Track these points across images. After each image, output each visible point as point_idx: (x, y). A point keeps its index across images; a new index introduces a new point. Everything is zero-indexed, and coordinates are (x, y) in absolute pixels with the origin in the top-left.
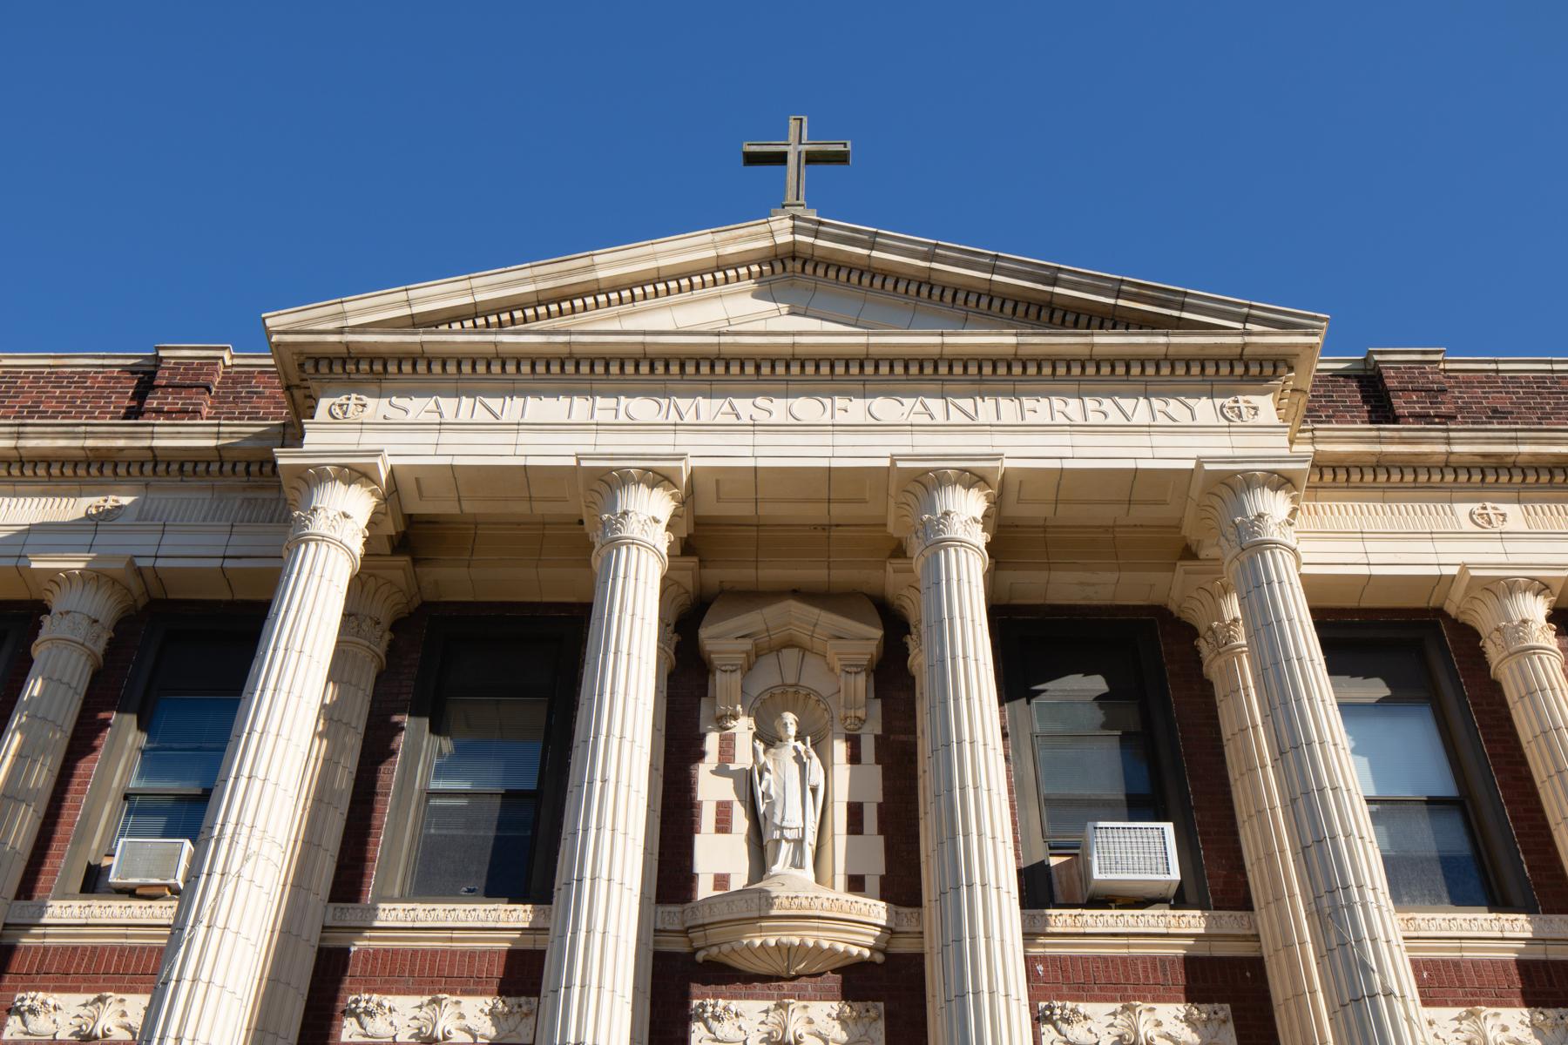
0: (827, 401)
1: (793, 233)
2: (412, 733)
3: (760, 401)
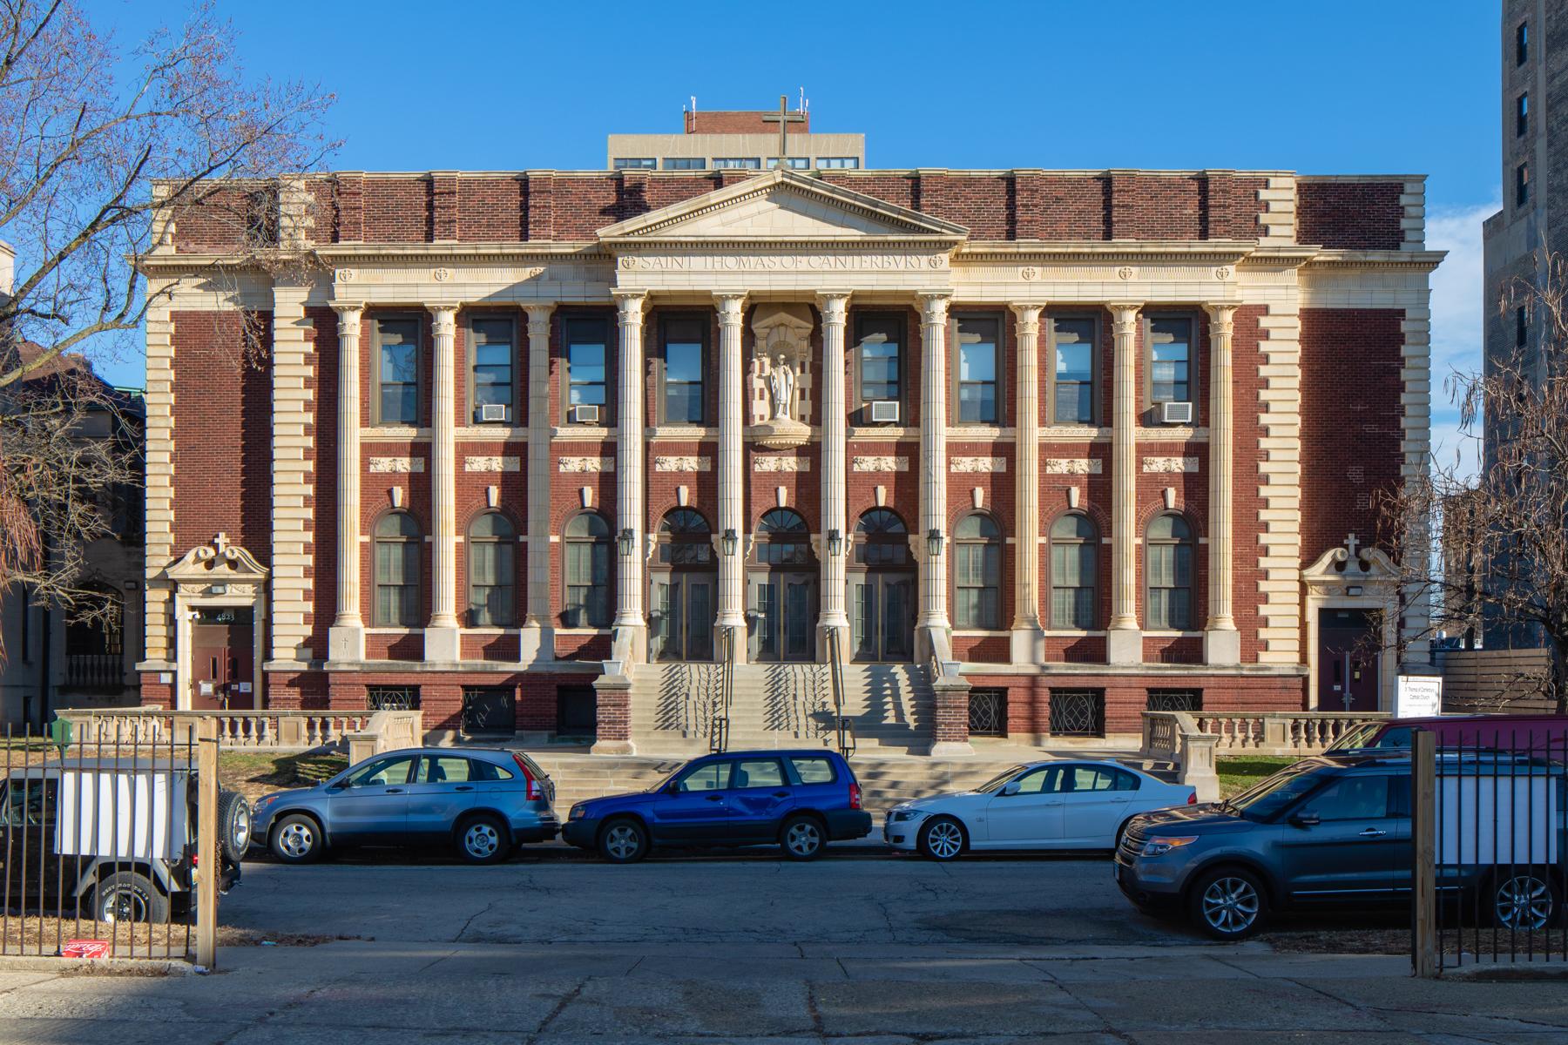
2: (656, 363)
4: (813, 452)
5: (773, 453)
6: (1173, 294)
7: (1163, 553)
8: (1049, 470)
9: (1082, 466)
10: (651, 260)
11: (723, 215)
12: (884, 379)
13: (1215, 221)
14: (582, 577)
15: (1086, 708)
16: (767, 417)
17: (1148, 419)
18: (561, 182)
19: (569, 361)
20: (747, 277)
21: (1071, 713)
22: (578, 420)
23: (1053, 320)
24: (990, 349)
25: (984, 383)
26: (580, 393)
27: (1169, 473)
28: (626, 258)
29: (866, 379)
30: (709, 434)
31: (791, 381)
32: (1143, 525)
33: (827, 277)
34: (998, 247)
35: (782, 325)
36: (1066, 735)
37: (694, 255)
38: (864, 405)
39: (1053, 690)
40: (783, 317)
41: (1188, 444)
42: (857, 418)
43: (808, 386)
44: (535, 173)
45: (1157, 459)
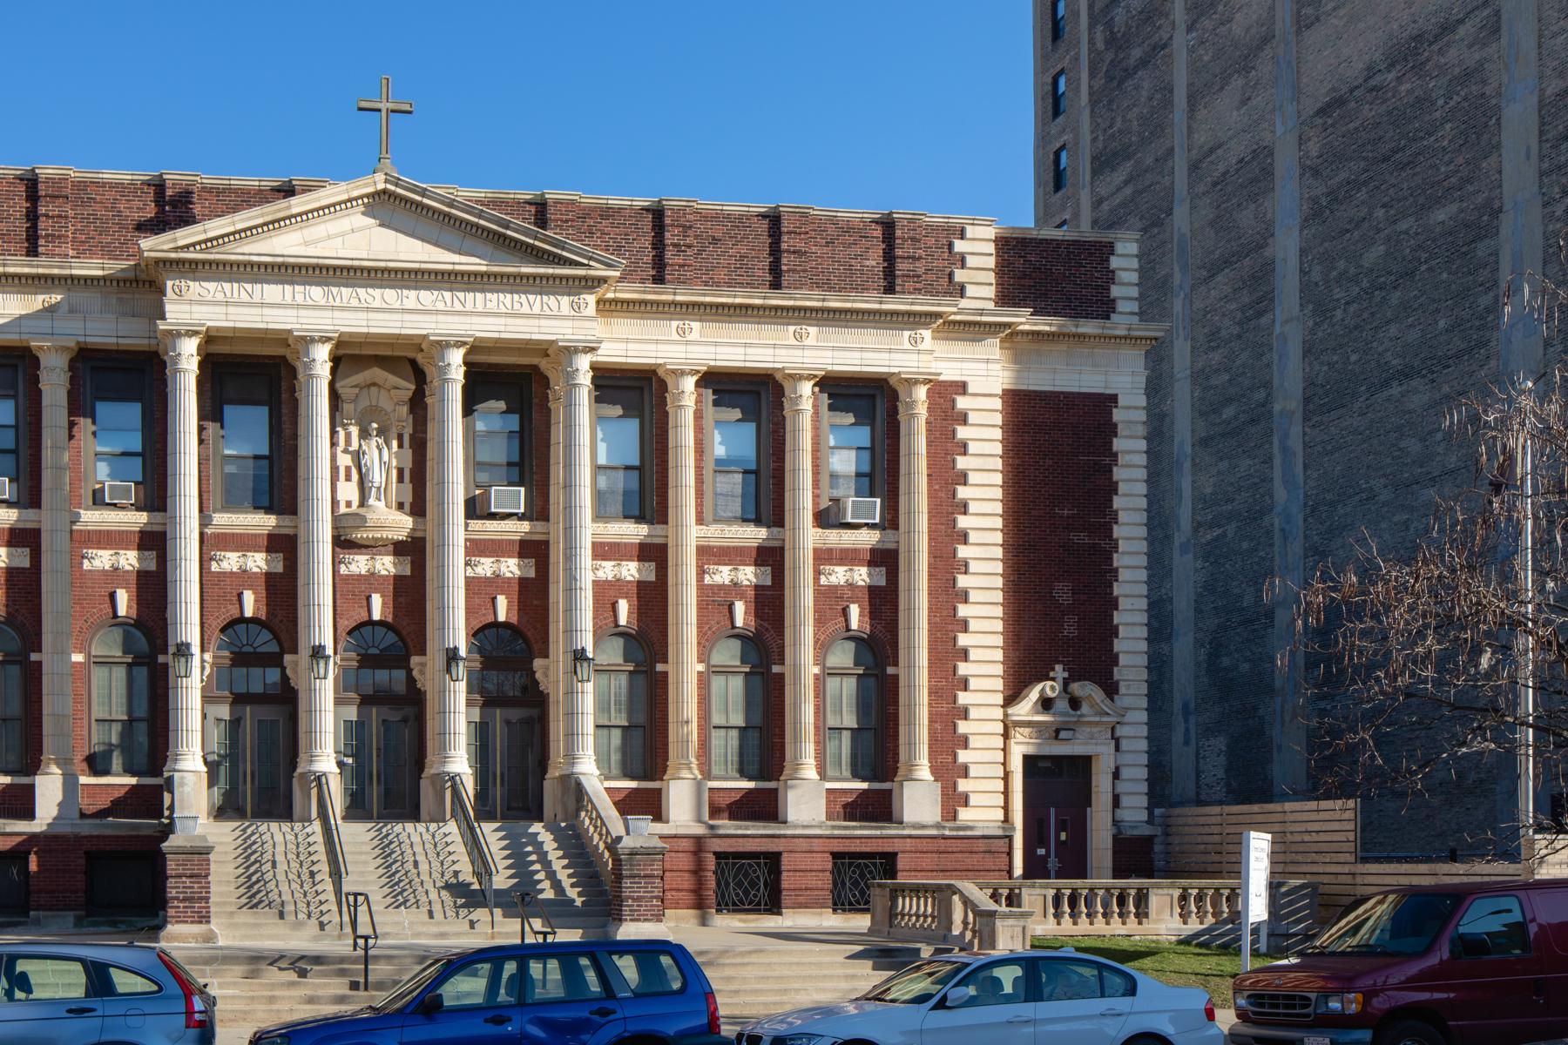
0: (399, 291)
1: (385, 182)
2: (211, 427)
3: (370, 290)
4: (413, 550)
5: (364, 550)
6: (858, 362)
7: (844, 685)
8: (707, 580)
9: (748, 575)
10: (212, 286)
11: (305, 231)
12: (502, 458)
13: (903, 276)
14: (114, 708)
15: (758, 877)
16: (355, 504)
17: (824, 519)
18: (81, 186)
19: (94, 423)
20: (337, 314)
21: (739, 884)
22: (107, 501)
23: (711, 391)
24: (633, 426)
25: (627, 468)
26: (109, 465)
27: (851, 586)
28: (177, 282)
29: (480, 458)
30: (281, 524)
31: (386, 458)
32: (822, 649)
33: (441, 318)
34: (650, 293)
35: (374, 384)
36: (734, 911)
37: (268, 282)
38: (477, 492)
39: (719, 855)
40: (376, 373)
41: (873, 551)
42: (475, 509)
43: (408, 465)
44: (46, 171)
45: (837, 569)
